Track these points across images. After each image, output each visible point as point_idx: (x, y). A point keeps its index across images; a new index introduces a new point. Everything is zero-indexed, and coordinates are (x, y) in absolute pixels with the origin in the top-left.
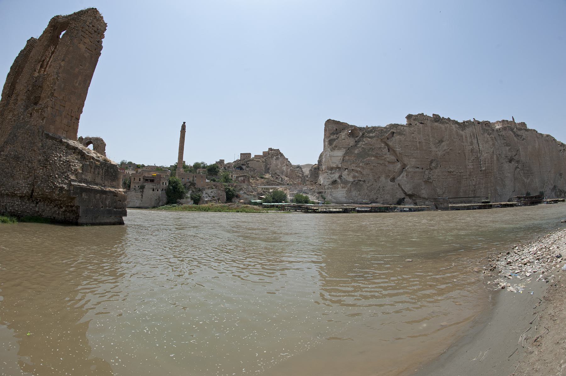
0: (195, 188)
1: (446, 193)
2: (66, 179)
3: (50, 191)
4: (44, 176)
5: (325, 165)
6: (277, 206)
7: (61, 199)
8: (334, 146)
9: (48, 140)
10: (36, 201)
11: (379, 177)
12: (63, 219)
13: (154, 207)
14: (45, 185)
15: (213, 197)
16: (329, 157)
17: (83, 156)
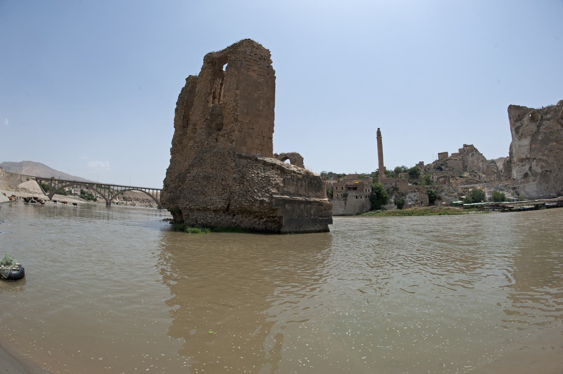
0: (398, 193)
2: (266, 193)
3: (249, 204)
4: (242, 192)
6: (477, 207)
7: (261, 210)
9: (241, 160)
10: (233, 213)
12: (263, 228)
13: (358, 214)
14: (243, 200)
15: (417, 201)
17: (282, 170)
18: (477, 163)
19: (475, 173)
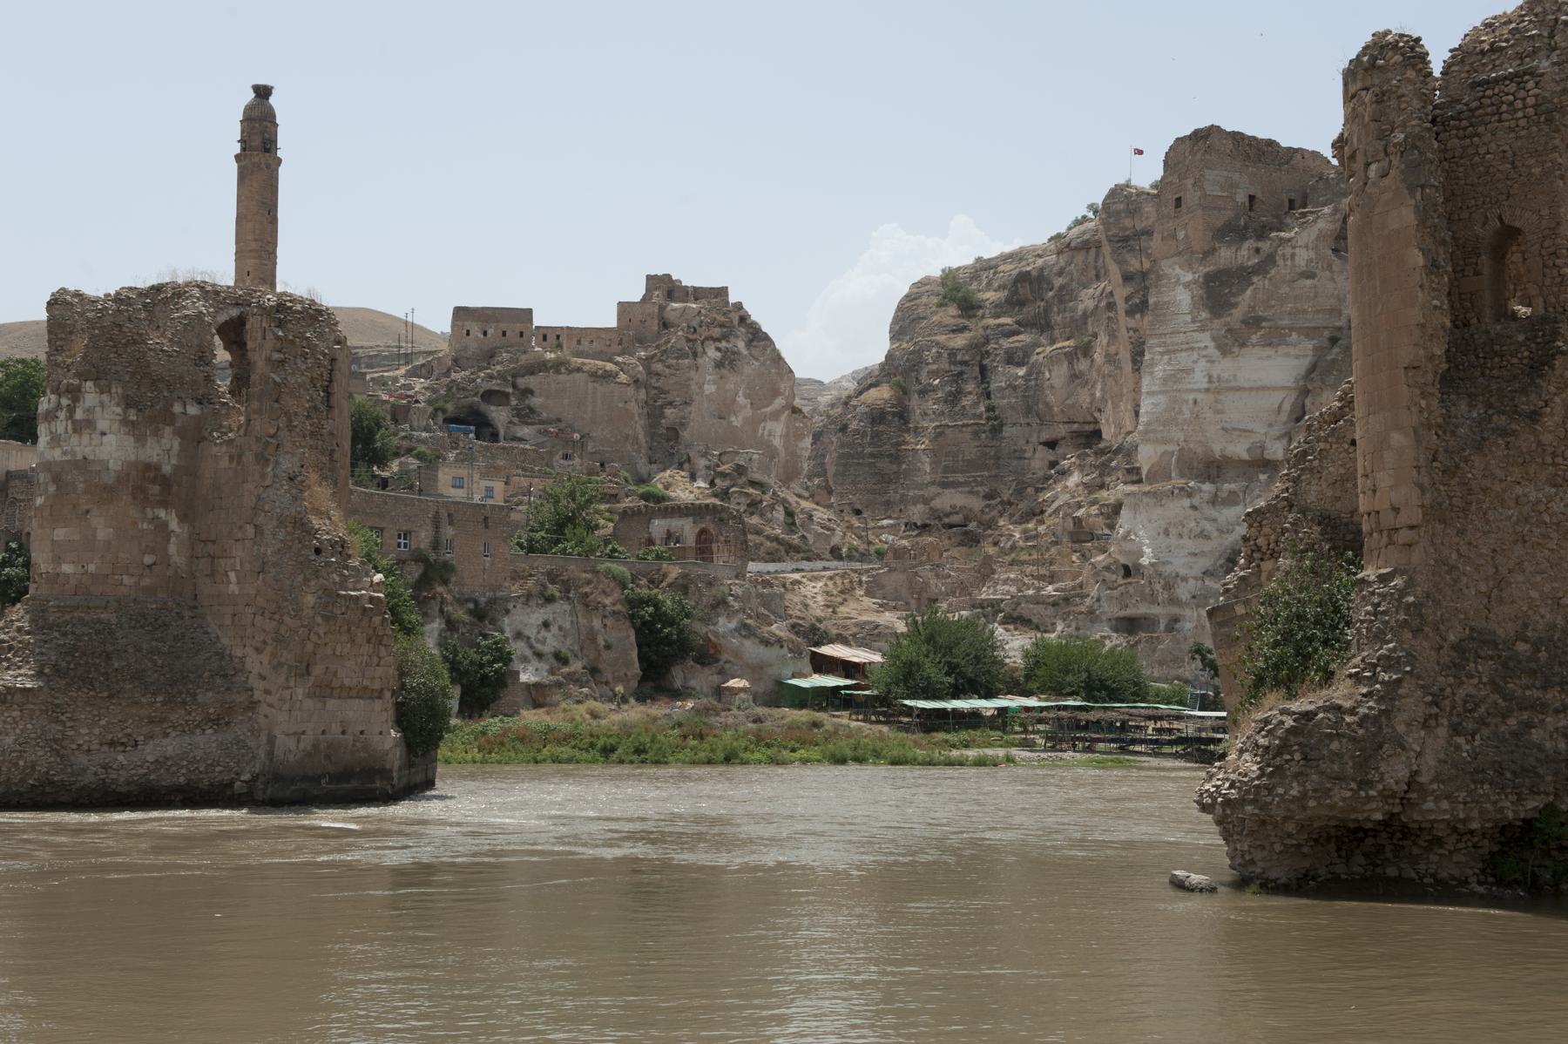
5: (1165, 441)
8: (1243, 322)
16: (1207, 390)
18: (755, 422)
19: (753, 484)
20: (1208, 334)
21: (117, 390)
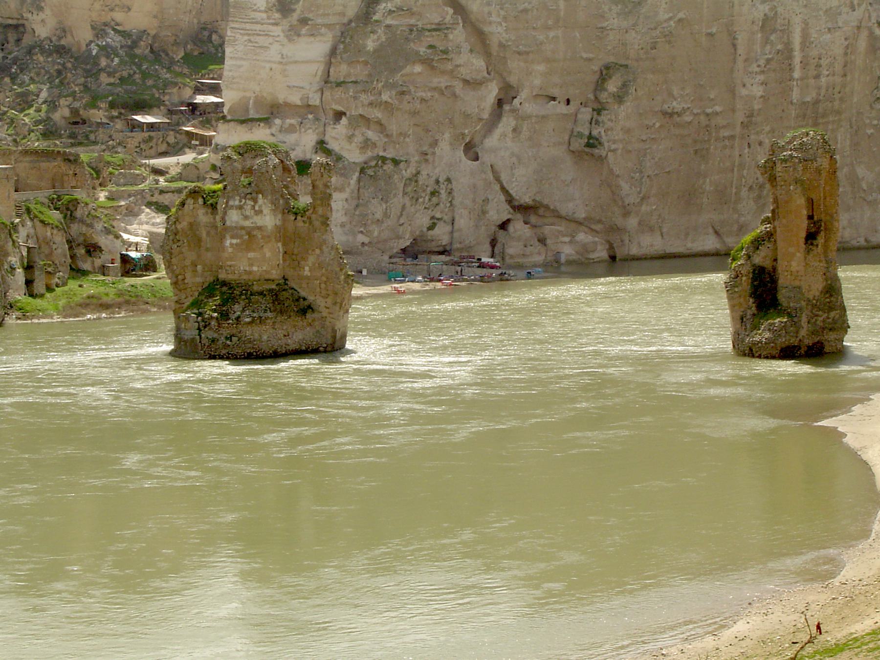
1: (652, 199)
5: (245, 90)
8: (298, 21)
11: (435, 143)
16: (281, 63)
20: (280, 28)
21: (269, 197)
